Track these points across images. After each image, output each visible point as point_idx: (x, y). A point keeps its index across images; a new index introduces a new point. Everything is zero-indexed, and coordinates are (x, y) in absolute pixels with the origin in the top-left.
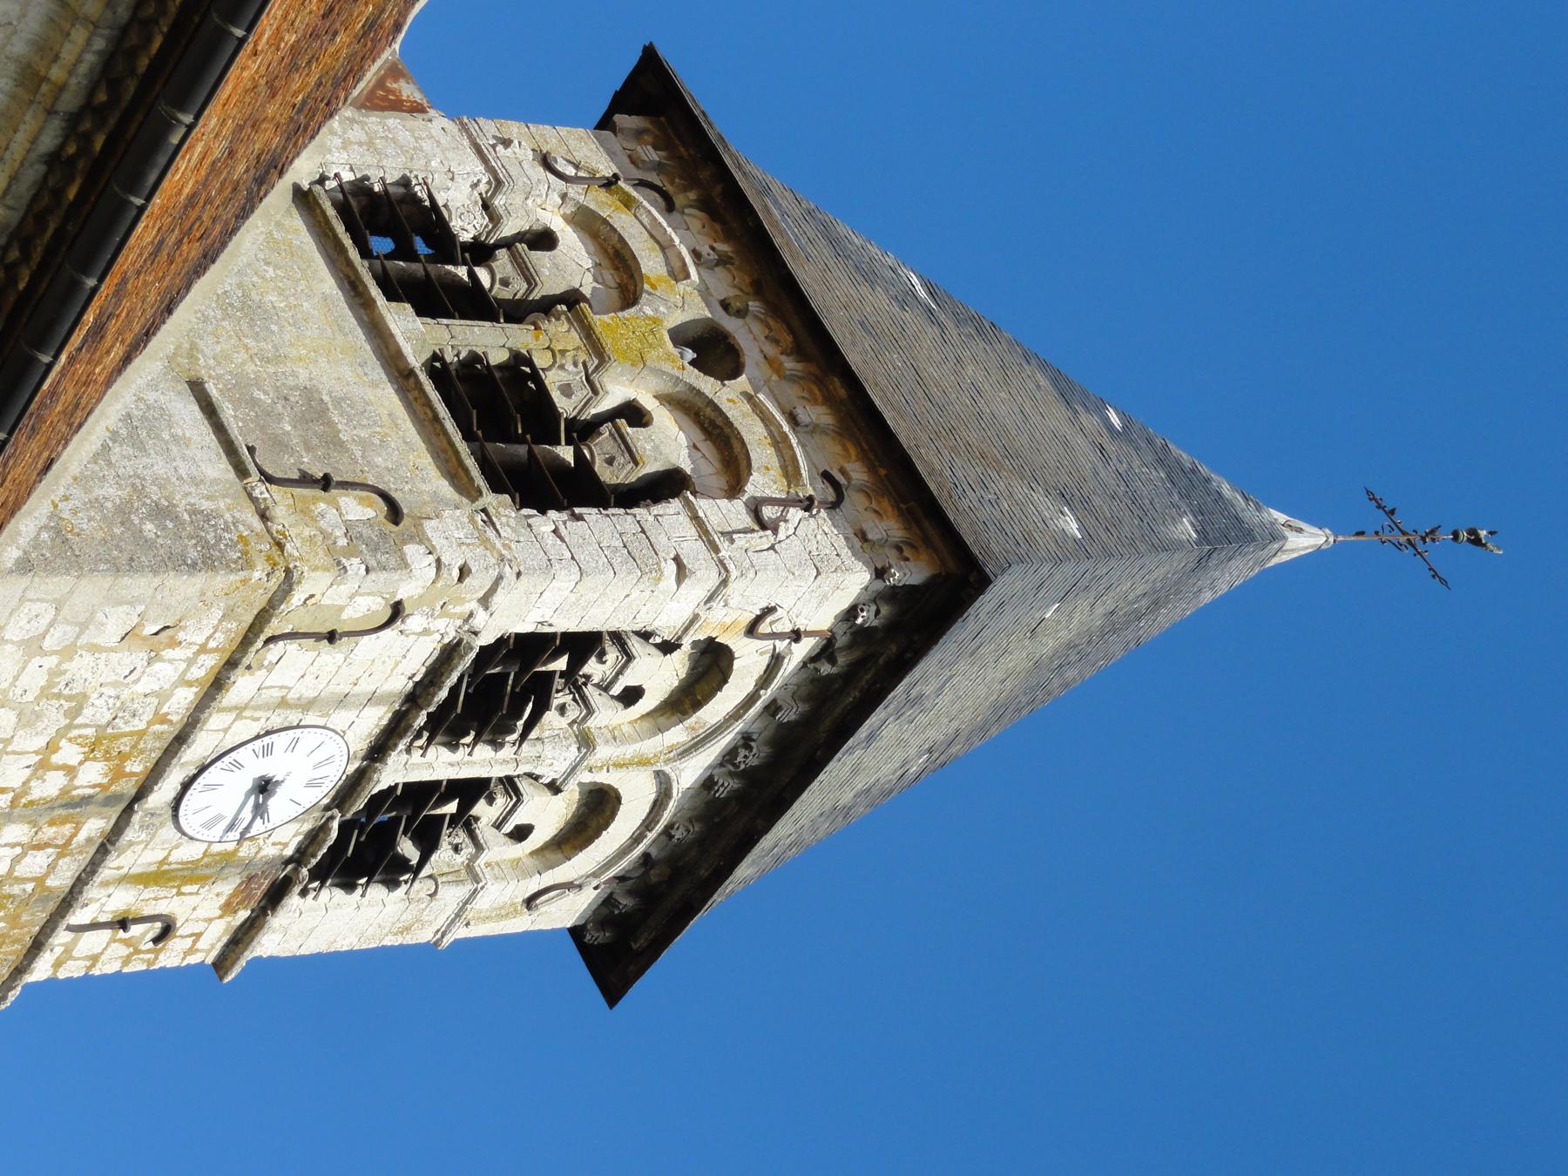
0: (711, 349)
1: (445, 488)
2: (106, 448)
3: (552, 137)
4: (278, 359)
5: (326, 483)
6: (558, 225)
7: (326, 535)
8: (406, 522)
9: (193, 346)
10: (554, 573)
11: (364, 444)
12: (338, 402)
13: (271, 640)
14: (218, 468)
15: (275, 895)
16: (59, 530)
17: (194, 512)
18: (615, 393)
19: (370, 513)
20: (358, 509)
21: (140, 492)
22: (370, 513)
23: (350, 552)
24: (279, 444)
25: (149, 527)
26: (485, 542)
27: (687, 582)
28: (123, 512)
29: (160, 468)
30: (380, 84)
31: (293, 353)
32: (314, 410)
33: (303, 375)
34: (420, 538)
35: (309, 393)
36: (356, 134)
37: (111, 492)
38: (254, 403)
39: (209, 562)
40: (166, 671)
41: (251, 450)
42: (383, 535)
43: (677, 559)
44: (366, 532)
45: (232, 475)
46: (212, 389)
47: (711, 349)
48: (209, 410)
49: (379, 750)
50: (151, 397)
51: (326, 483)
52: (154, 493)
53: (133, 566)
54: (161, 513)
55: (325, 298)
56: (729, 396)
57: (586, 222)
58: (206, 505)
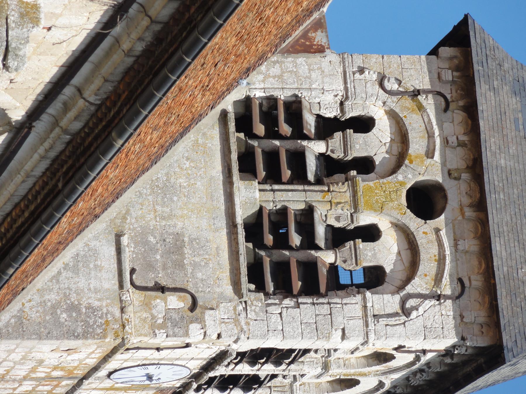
0: (424, 201)
1: (229, 290)
2: (59, 273)
3: (393, 64)
4: (170, 216)
5: (162, 289)
7: (153, 317)
8: (198, 310)
9: (128, 212)
10: (282, 323)
11: (195, 265)
12: (191, 241)
13: (128, 349)
14: (112, 283)
17: (89, 307)
18: (365, 219)
19: (182, 305)
20: (174, 302)
21: (66, 297)
22: (182, 305)
23: (162, 326)
24: (150, 266)
25: (64, 315)
26: (236, 322)
27: (345, 341)
28: (54, 307)
29: (82, 283)
30: (305, 35)
31: (179, 213)
32: (176, 246)
33: (180, 225)
34: (201, 320)
35: (178, 237)
36: (276, 70)
37: (53, 297)
38: (146, 243)
39: (85, 336)
41: (133, 271)
42: (182, 318)
43: (343, 330)
44: (175, 316)
45: (117, 287)
46: (125, 240)
47: (424, 201)
48: (119, 251)
50: (92, 244)
51: (162, 289)
52: (74, 298)
53: (49, 336)
54: (73, 308)
55: (212, 178)
56: (421, 229)
57: (392, 115)
58: (96, 304)
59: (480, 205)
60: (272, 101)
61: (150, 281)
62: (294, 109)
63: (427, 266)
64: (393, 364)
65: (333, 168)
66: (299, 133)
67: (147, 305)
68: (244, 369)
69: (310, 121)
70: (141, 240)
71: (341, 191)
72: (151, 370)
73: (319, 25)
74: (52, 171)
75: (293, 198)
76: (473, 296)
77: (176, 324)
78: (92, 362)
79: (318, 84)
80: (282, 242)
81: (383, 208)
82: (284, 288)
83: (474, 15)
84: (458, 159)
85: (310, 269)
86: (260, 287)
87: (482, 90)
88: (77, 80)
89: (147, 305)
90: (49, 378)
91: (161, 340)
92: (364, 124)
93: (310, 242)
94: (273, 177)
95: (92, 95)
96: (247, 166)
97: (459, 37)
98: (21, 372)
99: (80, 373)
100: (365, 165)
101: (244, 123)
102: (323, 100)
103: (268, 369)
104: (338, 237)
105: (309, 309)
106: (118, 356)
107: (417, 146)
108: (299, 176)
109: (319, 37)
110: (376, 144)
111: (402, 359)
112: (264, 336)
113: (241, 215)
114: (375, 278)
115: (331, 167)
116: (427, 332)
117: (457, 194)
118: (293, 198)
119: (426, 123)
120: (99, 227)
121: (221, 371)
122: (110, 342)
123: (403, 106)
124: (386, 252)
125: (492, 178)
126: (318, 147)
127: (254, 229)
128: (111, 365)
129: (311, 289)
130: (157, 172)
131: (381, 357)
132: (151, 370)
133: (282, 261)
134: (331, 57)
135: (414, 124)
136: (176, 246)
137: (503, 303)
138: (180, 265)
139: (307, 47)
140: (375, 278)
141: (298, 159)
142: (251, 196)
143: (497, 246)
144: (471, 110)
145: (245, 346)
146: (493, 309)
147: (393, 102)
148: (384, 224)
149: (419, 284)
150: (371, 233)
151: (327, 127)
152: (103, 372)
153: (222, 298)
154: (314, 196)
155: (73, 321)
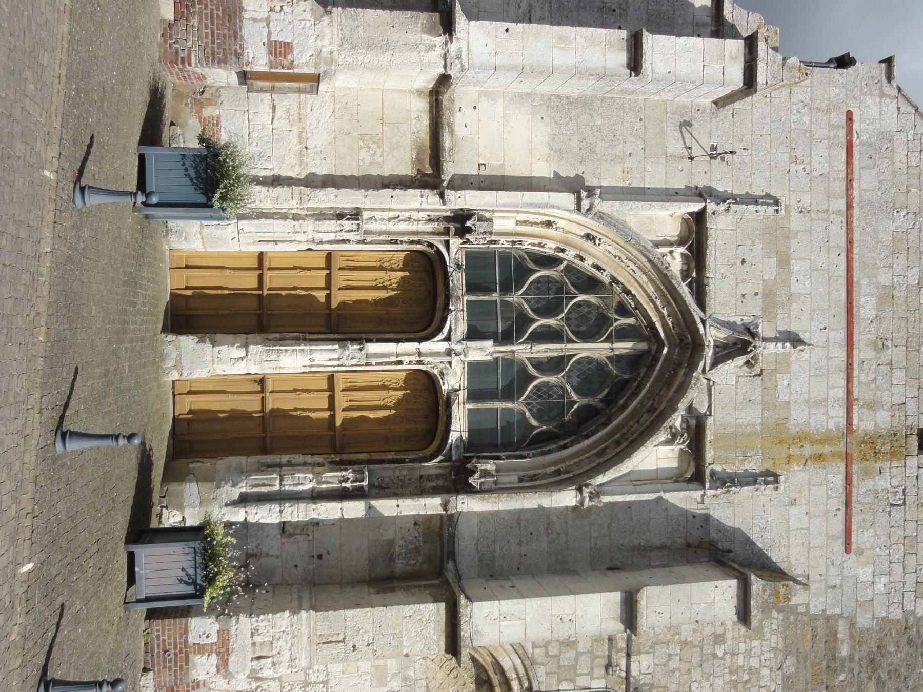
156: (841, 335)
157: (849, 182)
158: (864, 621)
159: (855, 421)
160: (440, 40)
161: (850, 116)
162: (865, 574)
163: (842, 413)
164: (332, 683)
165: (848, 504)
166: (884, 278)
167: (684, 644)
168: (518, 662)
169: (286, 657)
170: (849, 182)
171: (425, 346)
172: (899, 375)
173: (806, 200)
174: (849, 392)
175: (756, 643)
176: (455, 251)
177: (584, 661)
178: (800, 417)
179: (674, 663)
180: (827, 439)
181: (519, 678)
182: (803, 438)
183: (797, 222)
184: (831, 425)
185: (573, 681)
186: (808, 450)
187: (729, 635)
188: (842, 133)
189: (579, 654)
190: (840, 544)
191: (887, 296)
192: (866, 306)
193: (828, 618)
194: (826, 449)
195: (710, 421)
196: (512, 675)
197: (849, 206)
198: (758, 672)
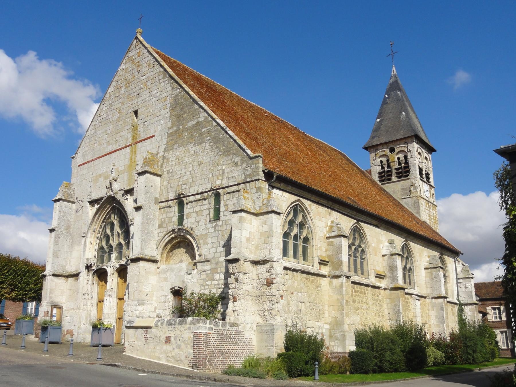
0: (392, 150)
3: (371, 158)
5: (410, 191)
6: (380, 160)
10: (415, 171)
15: (431, 186)
16: (417, 213)
18: (396, 160)
20: (412, 188)
24: (407, 193)
32: (403, 189)
35: (402, 189)
37: (413, 208)
39: (419, 202)
40: (423, 203)
47: (392, 150)
49: (424, 182)
51: (410, 191)
54: (414, 205)
56: (397, 150)
57: (379, 158)
59: (392, 142)
60: (379, 177)
61: (408, 192)
62: (380, 173)
63: (402, 149)
64: (421, 152)
65: (389, 166)
66: (384, 172)
67: (413, 193)
68: (424, 176)
69: (382, 170)
70: (403, 195)
71: (392, 164)
72: (425, 191)
73: (366, 171)
74: (365, 215)
75: (394, 172)
76: (407, 141)
77: (416, 188)
78: (424, 201)
79: (376, 170)
80: (401, 172)
81: (395, 157)
82: (409, 171)
83: (363, 146)
84: (385, 146)
85: (405, 167)
86: (408, 175)
87: (373, 144)
88: (347, 214)
89: (413, 193)
90: (429, 207)
91: (418, 190)
92: (381, 162)
93: (401, 168)
94: (391, 175)
95: (349, 211)
96: (390, 179)
97: (366, 148)
98: (428, 212)
99: (427, 202)
100: (388, 161)
101: (383, 181)
102: (378, 169)
103: (424, 172)
104: (400, 164)
105: (411, 167)
106: (423, 196)
107: (384, 153)
108: (390, 171)
109: (368, 171)
110: (384, 160)
111: (419, 150)
112: (416, 174)
113: (397, 180)
114: (406, 157)
115: (389, 166)
116: (413, 147)
117: (391, 146)
118: (394, 172)
119: (380, 152)
120: (401, 202)
121: (425, 180)
122: (419, 198)
123: (378, 156)
124: (401, 156)
125: (387, 140)
126: (386, 168)
127: (399, 177)
128: (425, 197)
129: (408, 167)
130: (392, 194)
131: (419, 153)
132: (425, 191)
133: (404, 172)
134: (371, 168)
135: (380, 154)
136: (403, 189)
137: (407, 136)
138: (406, 188)
139: (370, 173)
140: (406, 157)
141: (388, 172)
142: (394, 178)
143: (398, 138)
144: (377, 145)
145: (419, 176)
146: (408, 137)
147: (377, 158)
148: (397, 157)
149: (406, 150)
150: (398, 158)
151: (383, 168)
152: (427, 199)
153: (411, 181)
154: (393, 168)
155: (417, 205)
156: (113, 154)
157: (89, 162)
158: (169, 124)
159: (129, 144)
160: (47, 278)
161: (79, 166)
162: (160, 128)
163: (127, 148)
164: (166, 294)
165: (144, 140)
166: (105, 145)
167: (169, 183)
168: (167, 236)
169: (135, 307)
170: (89, 162)
171: (109, 274)
172: (122, 134)
173: (91, 173)
174: (124, 148)
175: (170, 159)
176: (94, 268)
177: (169, 215)
178: (127, 162)
179: (172, 185)
180: (132, 151)
181: (171, 235)
182: (131, 159)
183: (94, 175)
184: (129, 151)
185: (172, 218)
186: (133, 157)
187: (168, 169)
188: (82, 166)
189: (167, 217)
190: (152, 139)
191: (108, 143)
192: (110, 149)
193: (168, 137)
194: (134, 151)
195: (126, 189)
196: (169, 238)
197: (93, 160)
198: (177, 156)
